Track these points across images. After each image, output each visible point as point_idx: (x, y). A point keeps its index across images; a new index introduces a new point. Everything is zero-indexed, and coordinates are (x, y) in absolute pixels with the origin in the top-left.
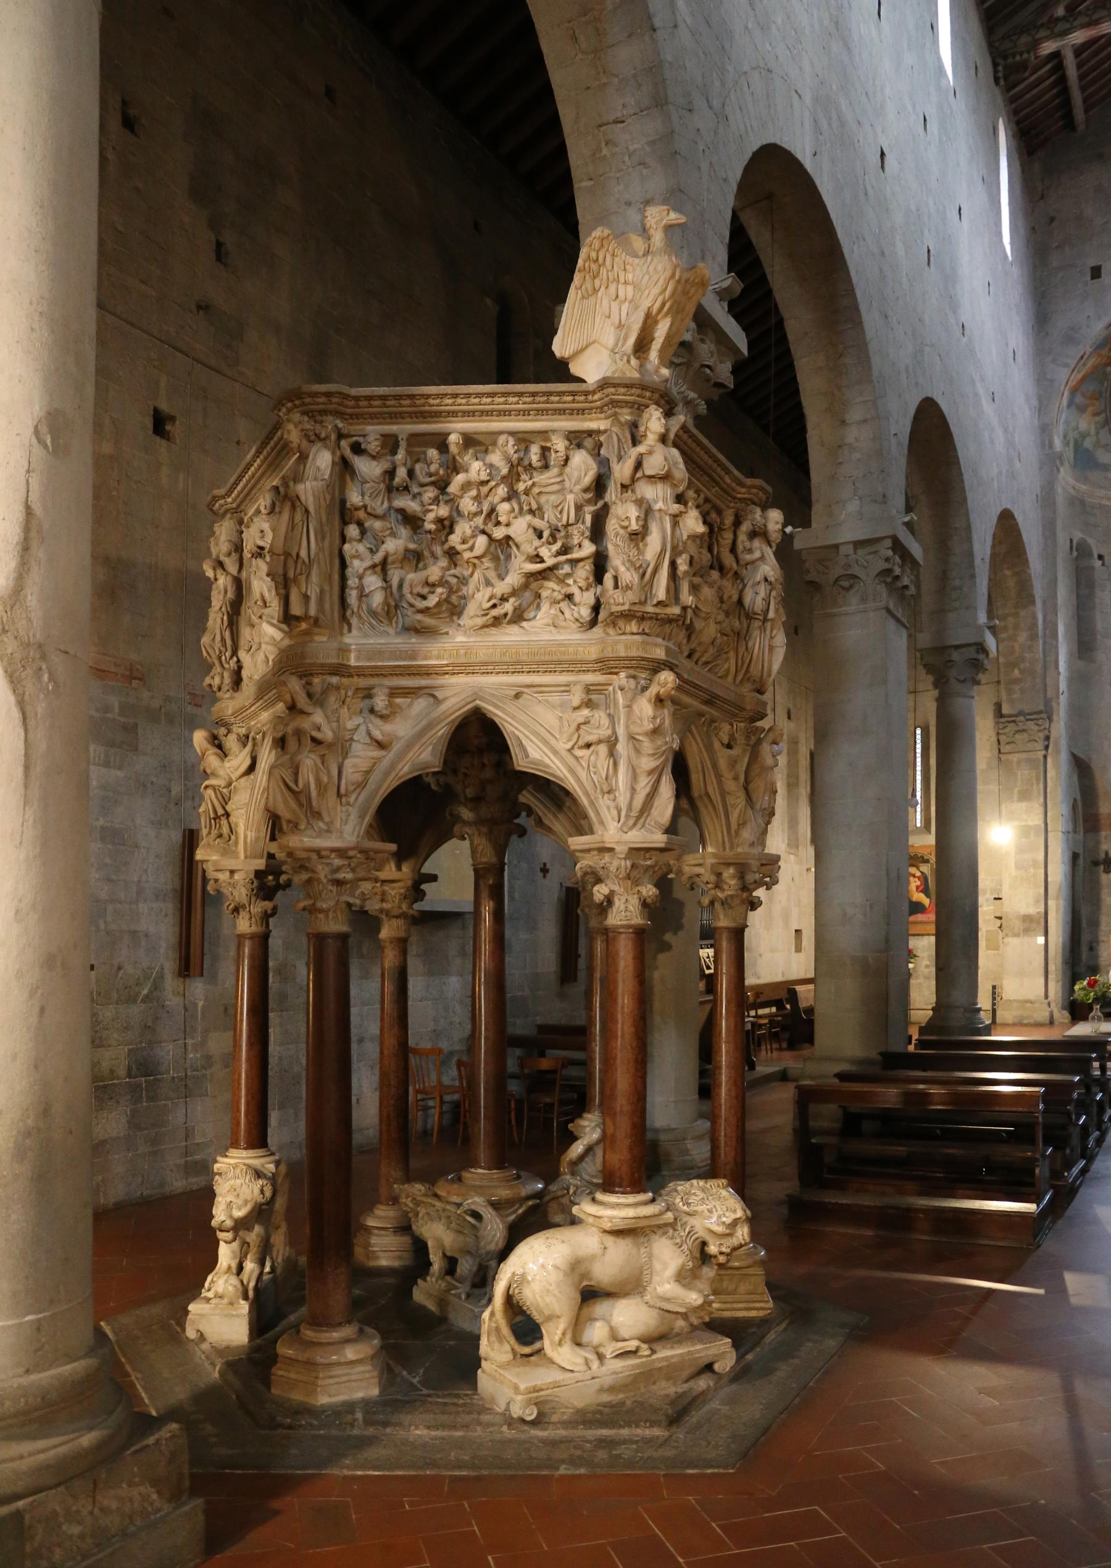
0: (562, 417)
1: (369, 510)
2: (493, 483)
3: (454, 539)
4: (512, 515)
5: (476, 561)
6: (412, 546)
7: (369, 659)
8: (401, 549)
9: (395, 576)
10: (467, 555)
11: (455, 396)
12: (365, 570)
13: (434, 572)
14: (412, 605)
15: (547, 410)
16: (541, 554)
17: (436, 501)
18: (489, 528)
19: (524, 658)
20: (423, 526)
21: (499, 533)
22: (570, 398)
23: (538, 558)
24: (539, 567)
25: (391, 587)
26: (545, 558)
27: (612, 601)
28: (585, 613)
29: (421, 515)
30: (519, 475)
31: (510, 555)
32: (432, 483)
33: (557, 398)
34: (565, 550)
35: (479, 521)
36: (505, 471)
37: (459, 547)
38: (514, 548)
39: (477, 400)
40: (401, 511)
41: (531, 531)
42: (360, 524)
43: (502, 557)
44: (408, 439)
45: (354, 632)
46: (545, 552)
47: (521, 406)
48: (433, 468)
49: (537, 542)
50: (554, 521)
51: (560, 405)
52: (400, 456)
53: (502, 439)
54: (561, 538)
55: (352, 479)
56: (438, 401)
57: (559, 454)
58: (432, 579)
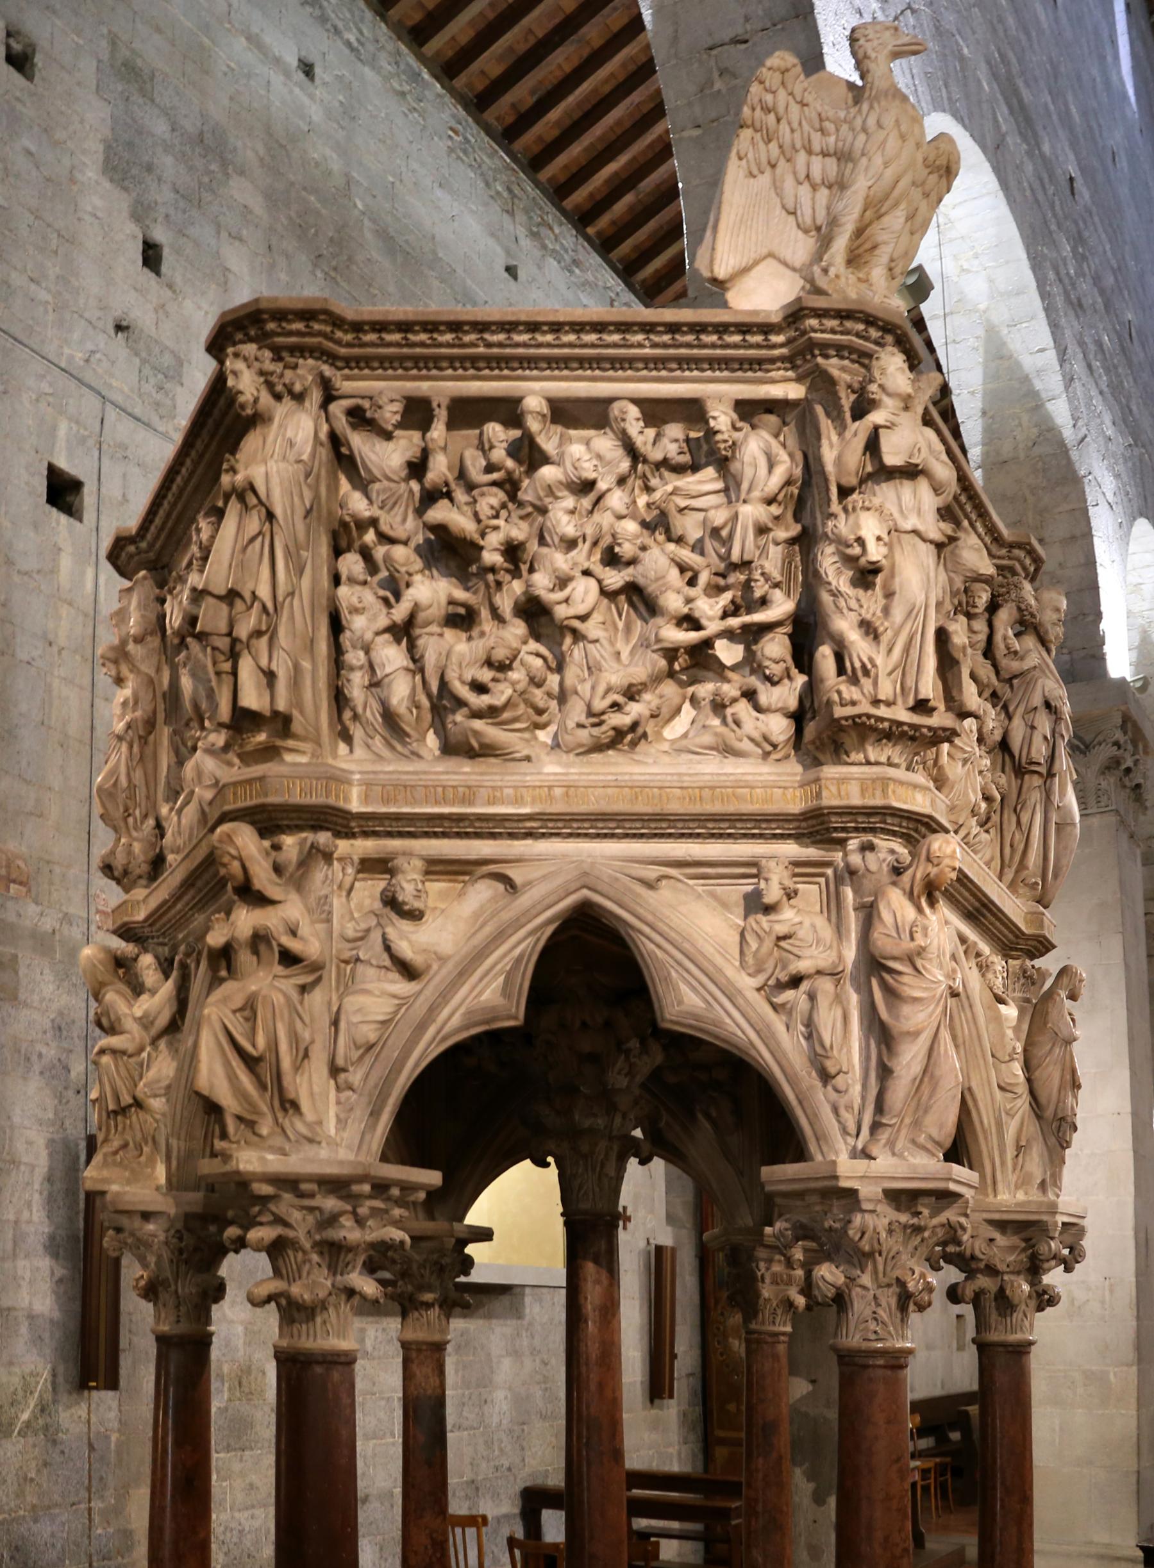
7: (386, 801)
12: (377, 634)
14: (460, 703)
16: (697, 614)
19: (675, 807)
20: (478, 559)
23: (690, 622)
24: (693, 636)
26: (704, 622)
27: (836, 697)
29: (476, 537)
42: (366, 555)
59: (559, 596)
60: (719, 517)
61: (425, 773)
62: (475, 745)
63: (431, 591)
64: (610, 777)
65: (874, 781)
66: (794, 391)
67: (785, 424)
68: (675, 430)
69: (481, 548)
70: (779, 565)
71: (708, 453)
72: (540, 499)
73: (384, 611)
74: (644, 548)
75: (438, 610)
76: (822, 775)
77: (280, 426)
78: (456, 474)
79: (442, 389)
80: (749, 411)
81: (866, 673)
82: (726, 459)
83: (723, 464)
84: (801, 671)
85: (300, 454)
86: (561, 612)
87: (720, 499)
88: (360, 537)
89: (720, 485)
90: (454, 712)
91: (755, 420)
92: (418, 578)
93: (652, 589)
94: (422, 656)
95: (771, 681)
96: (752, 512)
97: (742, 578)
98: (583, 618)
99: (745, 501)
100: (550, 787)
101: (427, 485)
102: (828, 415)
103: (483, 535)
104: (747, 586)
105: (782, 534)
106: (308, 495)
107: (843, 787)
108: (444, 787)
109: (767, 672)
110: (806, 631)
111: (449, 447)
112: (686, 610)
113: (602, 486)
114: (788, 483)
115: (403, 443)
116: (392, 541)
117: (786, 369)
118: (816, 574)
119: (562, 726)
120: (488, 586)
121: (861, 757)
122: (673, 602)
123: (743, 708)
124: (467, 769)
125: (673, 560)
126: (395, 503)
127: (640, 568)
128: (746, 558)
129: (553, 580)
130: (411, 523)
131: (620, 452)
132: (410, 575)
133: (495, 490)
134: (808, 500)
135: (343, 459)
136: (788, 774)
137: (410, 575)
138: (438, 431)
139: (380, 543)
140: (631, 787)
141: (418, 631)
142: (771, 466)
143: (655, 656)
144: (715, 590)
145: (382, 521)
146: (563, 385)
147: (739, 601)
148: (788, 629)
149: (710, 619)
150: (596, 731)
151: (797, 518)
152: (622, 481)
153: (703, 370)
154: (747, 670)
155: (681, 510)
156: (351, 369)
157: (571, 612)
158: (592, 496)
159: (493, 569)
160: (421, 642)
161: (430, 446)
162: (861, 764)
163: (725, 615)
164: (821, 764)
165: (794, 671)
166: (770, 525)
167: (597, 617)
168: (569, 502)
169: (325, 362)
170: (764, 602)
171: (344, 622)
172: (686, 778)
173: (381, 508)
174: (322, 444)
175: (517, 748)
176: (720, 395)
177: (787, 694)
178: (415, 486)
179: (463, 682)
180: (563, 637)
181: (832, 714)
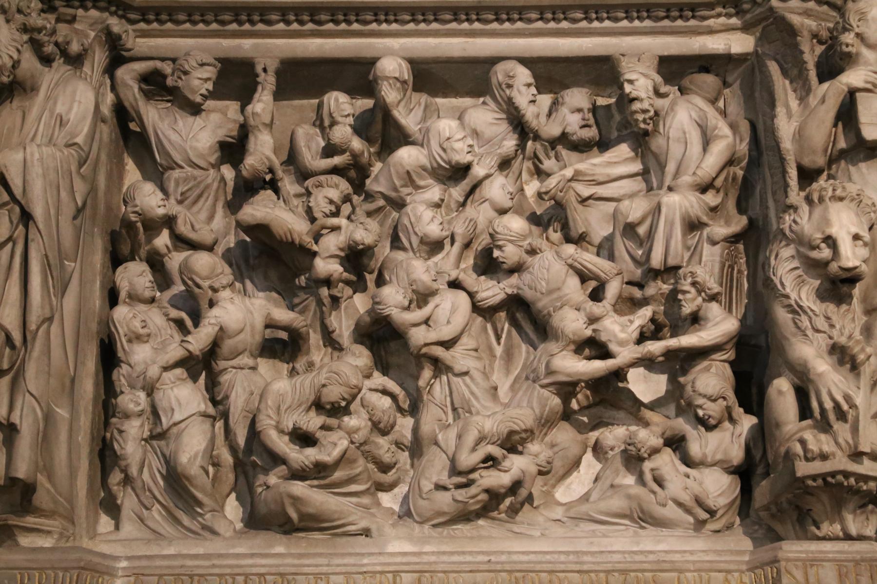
12: (166, 369)
14: (276, 459)
16: (603, 338)
20: (310, 267)
25: (225, 416)
26: (613, 347)
28: (718, 487)
29: (308, 240)
32: (335, 171)
42: (156, 263)
45: (129, 528)
53: (500, 72)
57: (636, 106)
58: (333, 393)
59: (417, 315)
60: (635, 209)
61: (220, 556)
62: (294, 515)
63: (242, 310)
64: (480, 558)
65: (857, 563)
66: (740, 43)
67: (726, 84)
68: (577, 97)
69: (315, 254)
70: (717, 269)
71: (621, 126)
72: (396, 190)
73: (178, 337)
74: (532, 252)
75: (252, 337)
76: (781, 555)
77: (48, 98)
78: (285, 157)
80: (675, 70)
81: (842, 416)
82: (646, 133)
83: (641, 140)
84: (746, 412)
86: (419, 336)
87: (637, 184)
88: (149, 240)
89: (637, 167)
90: (266, 471)
91: (686, 82)
92: (225, 294)
93: (542, 304)
94: (227, 397)
95: (706, 424)
96: (679, 202)
97: (666, 288)
98: (448, 344)
99: (670, 189)
100: (396, 573)
101: (245, 173)
102: (785, 73)
103: (317, 237)
104: (673, 298)
105: (720, 230)
107: (812, 572)
108: (247, 576)
109: (701, 413)
110: (754, 359)
111: (276, 122)
112: (588, 333)
113: (479, 171)
114: (731, 162)
115: (215, 117)
116: (194, 246)
117: (729, 16)
118: (768, 283)
119: (416, 487)
120: (320, 303)
121: (837, 528)
122: (572, 322)
123: (666, 462)
124: (280, 549)
125: (571, 266)
126: (200, 196)
127: (526, 277)
128: (671, 262)
129: (410, 295)
130: (220, 220)
132: (215, 290)
133: (336, 179)
134: (756, 183)
135: (130, 136)
136: (731, 552)
137: (215, 290)
138: (262, 104)
139: (176, 248)
140: (510, 572)
142: (706, 143)
143: (545, 393)
145: (180, 221)
146: (432, 41)
147: (661, 318)
148: (730, 355)
149: (622, 343)
150: (461, 495)
151: (741, 208)
152: (505, 164)
153: (616, 20)
154: (672, 409)
155: (584, 201)
156: (148, 22)
157: (433, 336)
158: (466, 184)
159: (328, 282)
160: (225, 378)
161: (252, 122)
162: (837, 538)
163: (642, 338)
164: (780, 539)
165: (738, 411)
166: (705, 219)
167: (467, 342)
168: (435, 192)
169: (112, 14)
170: (696, 320)
171: (120, 354)
172: (586, 558)
173: (180, 202)
174: (104, 121)
175: (350, 519)
176: (637, 49)
177: (729, 442)
178: (228, 172)
179: (281, 432)
180: (421, 368)
181: (793, 472)
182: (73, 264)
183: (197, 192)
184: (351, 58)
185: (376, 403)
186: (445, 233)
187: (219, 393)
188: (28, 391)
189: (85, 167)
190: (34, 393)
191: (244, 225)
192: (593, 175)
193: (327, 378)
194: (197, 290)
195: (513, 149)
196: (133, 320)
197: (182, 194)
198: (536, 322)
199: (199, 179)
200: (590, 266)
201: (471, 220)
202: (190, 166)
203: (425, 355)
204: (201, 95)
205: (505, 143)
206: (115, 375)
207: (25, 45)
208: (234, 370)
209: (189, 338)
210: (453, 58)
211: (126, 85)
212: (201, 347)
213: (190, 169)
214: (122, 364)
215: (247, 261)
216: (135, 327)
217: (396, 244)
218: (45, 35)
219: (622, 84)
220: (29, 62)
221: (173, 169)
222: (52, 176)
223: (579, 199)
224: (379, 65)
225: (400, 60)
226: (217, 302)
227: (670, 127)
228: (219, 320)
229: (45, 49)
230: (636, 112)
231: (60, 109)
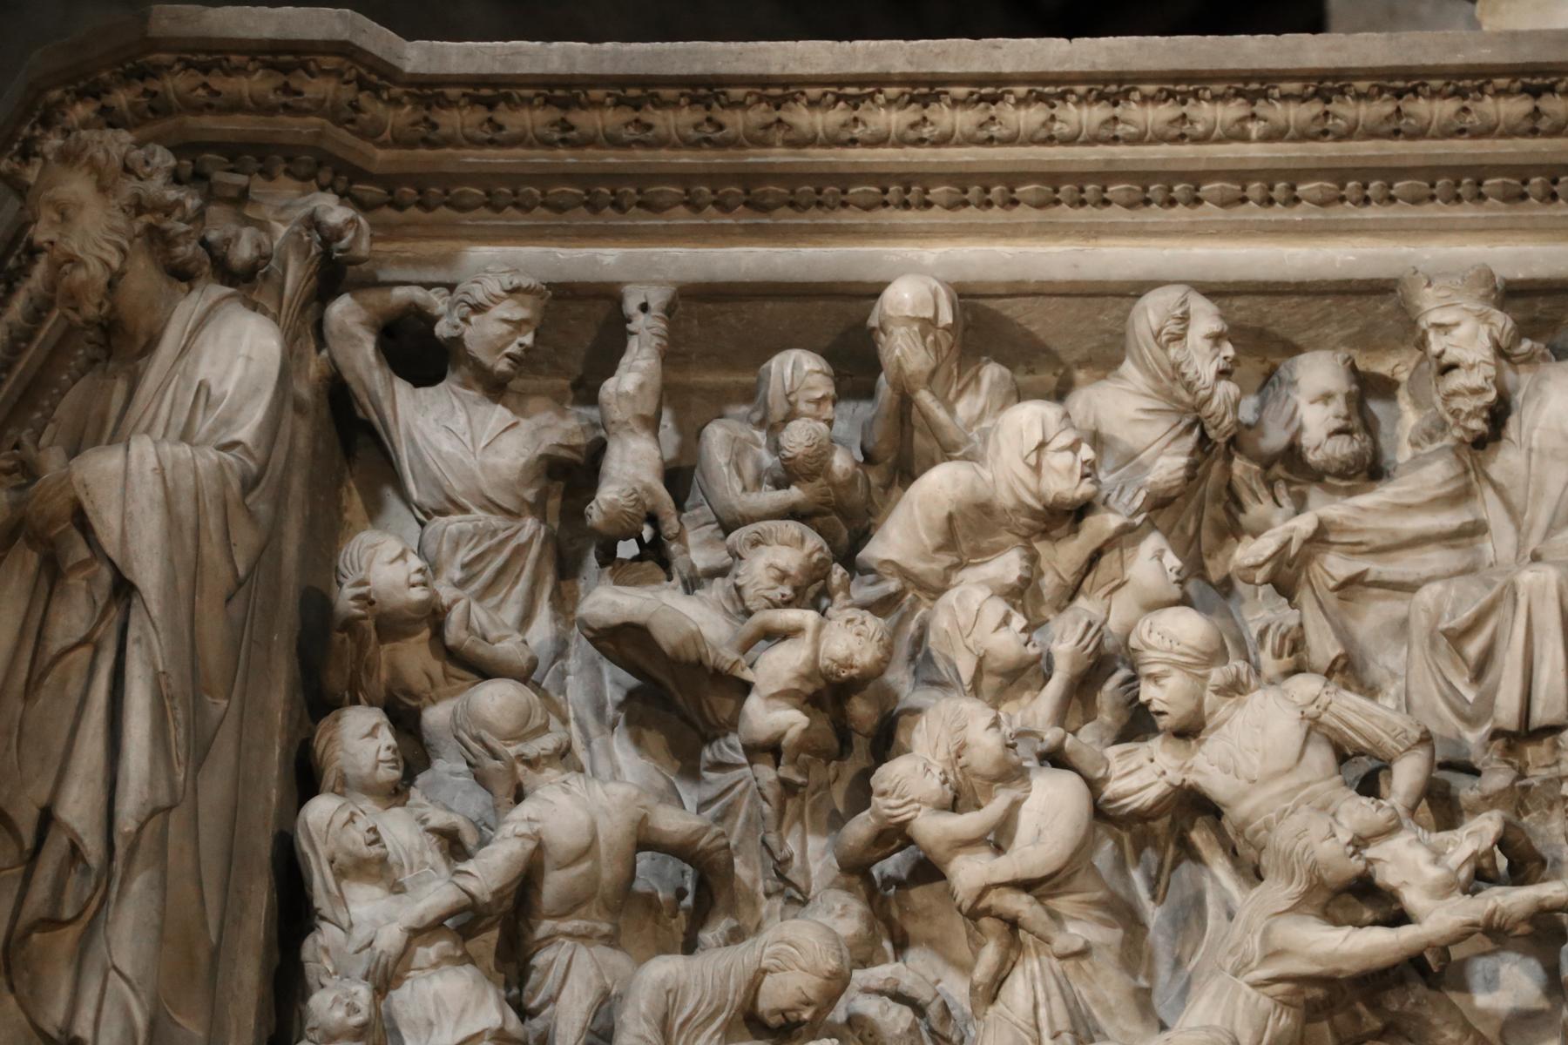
0: (1466, 212)
1: (454, 633)
2: (1113, 522)
3: (909, 781)
4: (1217, 675)
5: (1020, 904)
6: (674, 821)
8: (614, 830)
9: (573, 973)
10: (970, 872)
11: (925, 89)
12: (420, 933)
13: (797, 946)
15: (1391, 173)
16: (1388, 876)
17: (811, 590)
18: (1086, 741)
21: (1141, 775)
22: (1514, 108)
23: (1364, 897)
24: (1370, 943)
26: (1413, 898)
30: (1233, 502)
31: (1199, 902)
32: (792, 513)
33: (1448, 107)
34: (1519, 860)
35: (1037, 709)
36: (1168, 465)
37: (932, 827)
38: (1220, 868)
39: (1033, 116)
40: (625, 642)
41: (1320, 756)
43: (1153, 914)
44: (669, 310)
46: (1413, 864)
47: (1255, 152)
48: (798, 437)
49: (1358, 812)
50: (1444, 722)
51: (1463, 148)
52: (634, 375)
53: (1152, 312)
54: (1490, 801)
55: (374, 510)
56: (836, 116)
57: (1456, 380)
69: (746, 688)
79: (647, 267)
85: (227, 422)
94: (553, 999)
99: (1536, 558)
106: (246, 539)
112: (1357, 865)
131: (1161, 426)
133: (793, 528)
141: (545, 928)
144: (1439, 805)
145: (455, 616)
156: (399, 206)
171: (321, 901)
182: (224, 703)
183: (499, 561)
184: (832, 284)
185: (879, 1019)
186: (1032, 651)
187: (535, 991)
188: (115, 968)
189: (256, 493)
190: (128, 971)
191: (596, 626)
192: (1360, 531)
193: (775, 956)
194: (491, 764)
195: (1181, 473)
196: (350, 827)
197: (464, 566)
198: (1234, 851)
199: (501, 536)
200: (1356, 721)
201: (1090, 625)
202: (482, 507)
203: (988, 912)
204: (508, 356)
205: (1162, 461)
206: (309, 949)
207: (138, 240)
208: (568, 943)
209: (469, 866)
210: (1050, 283)
211: (352, 336)
212: (495, 886)
213: (480, 514)
214: (324, 925)
215: (600, 711)
216: (354, 842)
217: (924, 675)
218: (179, 220)
219: (1425, 333)
220: (143, 277)
221: (443, 513)
222: (185, 507)
223: (1332, 584)
224: (889, 293)
225: (935, 284)
226: (534, 789)
227: (1533, 428)
228: (536, 826)
229: (180, 250)
230: (1455, 394)
231: (205, 370)
